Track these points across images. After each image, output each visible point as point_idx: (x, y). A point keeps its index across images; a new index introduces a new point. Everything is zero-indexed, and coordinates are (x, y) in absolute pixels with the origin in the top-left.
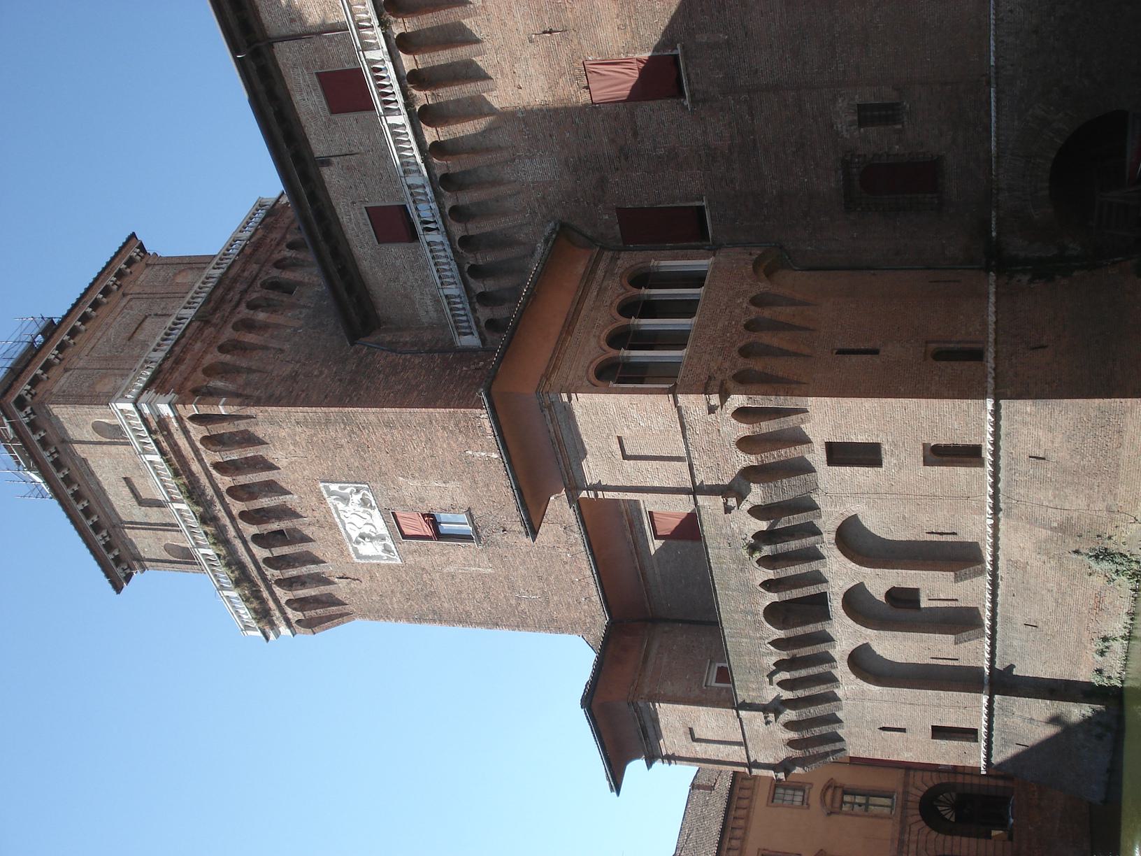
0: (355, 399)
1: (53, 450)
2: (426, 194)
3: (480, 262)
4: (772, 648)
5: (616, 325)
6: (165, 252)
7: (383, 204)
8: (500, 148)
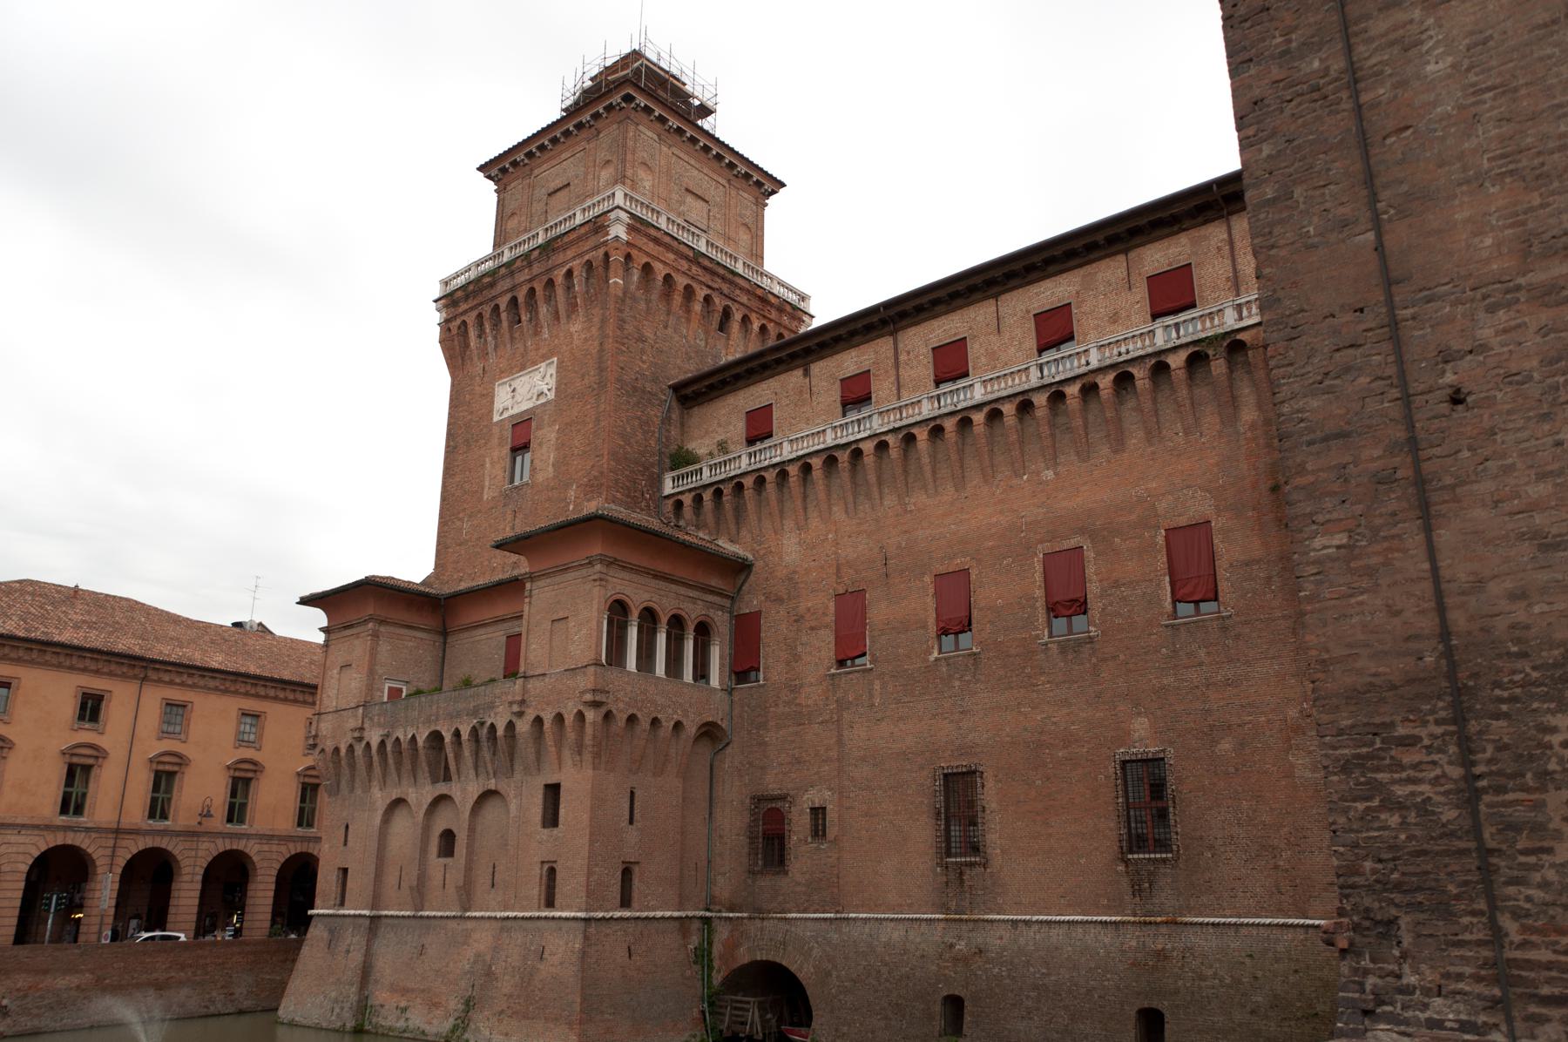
1: (592, 123)
2: (776, 456)
3: (724, 499)
4: (410, 736)
5: (661, 613)
6: (769, 213)
7: (774, 418)
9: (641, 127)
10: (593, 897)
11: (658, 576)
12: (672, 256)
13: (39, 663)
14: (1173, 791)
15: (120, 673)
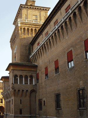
5: (23, 76)
11: (22, 70)
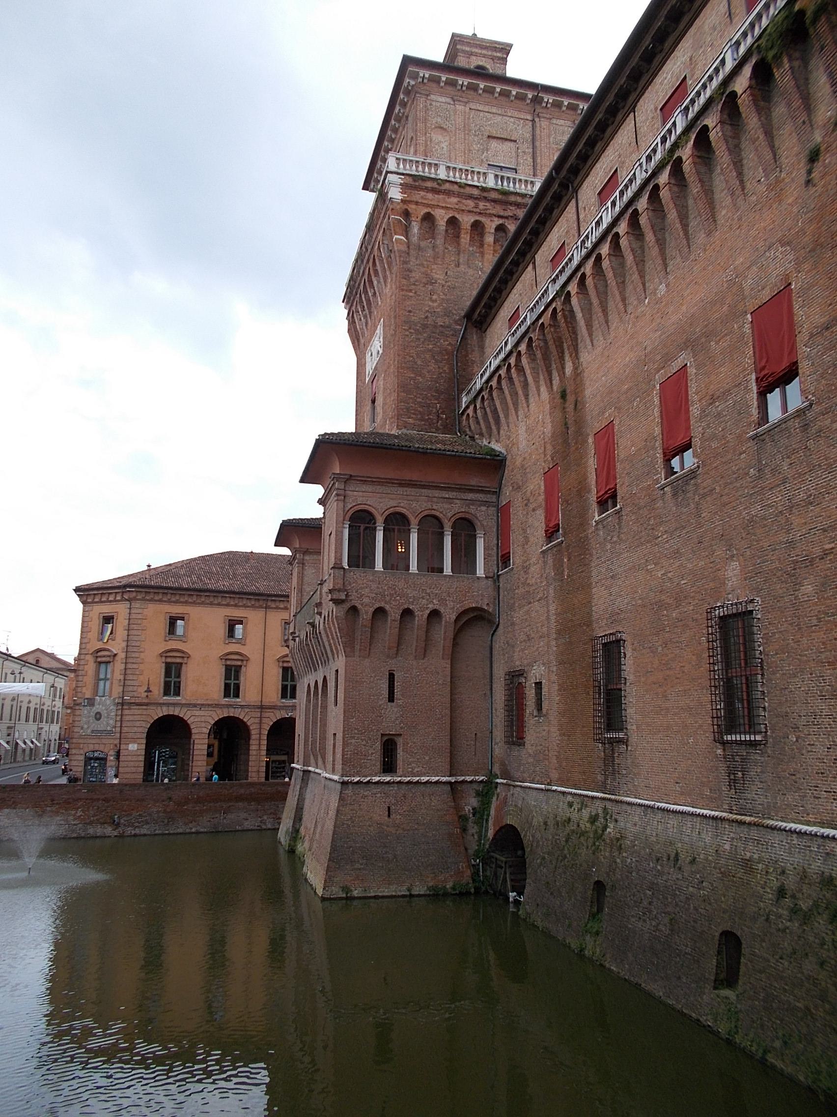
0: (407, 333)
8: (528, 406)
9: (432, 97)
10: (349, 763)
11: (402, 484)
12: (454, 200)
13: (199, 603)
14: (761, 653)
15: (250, 605)
